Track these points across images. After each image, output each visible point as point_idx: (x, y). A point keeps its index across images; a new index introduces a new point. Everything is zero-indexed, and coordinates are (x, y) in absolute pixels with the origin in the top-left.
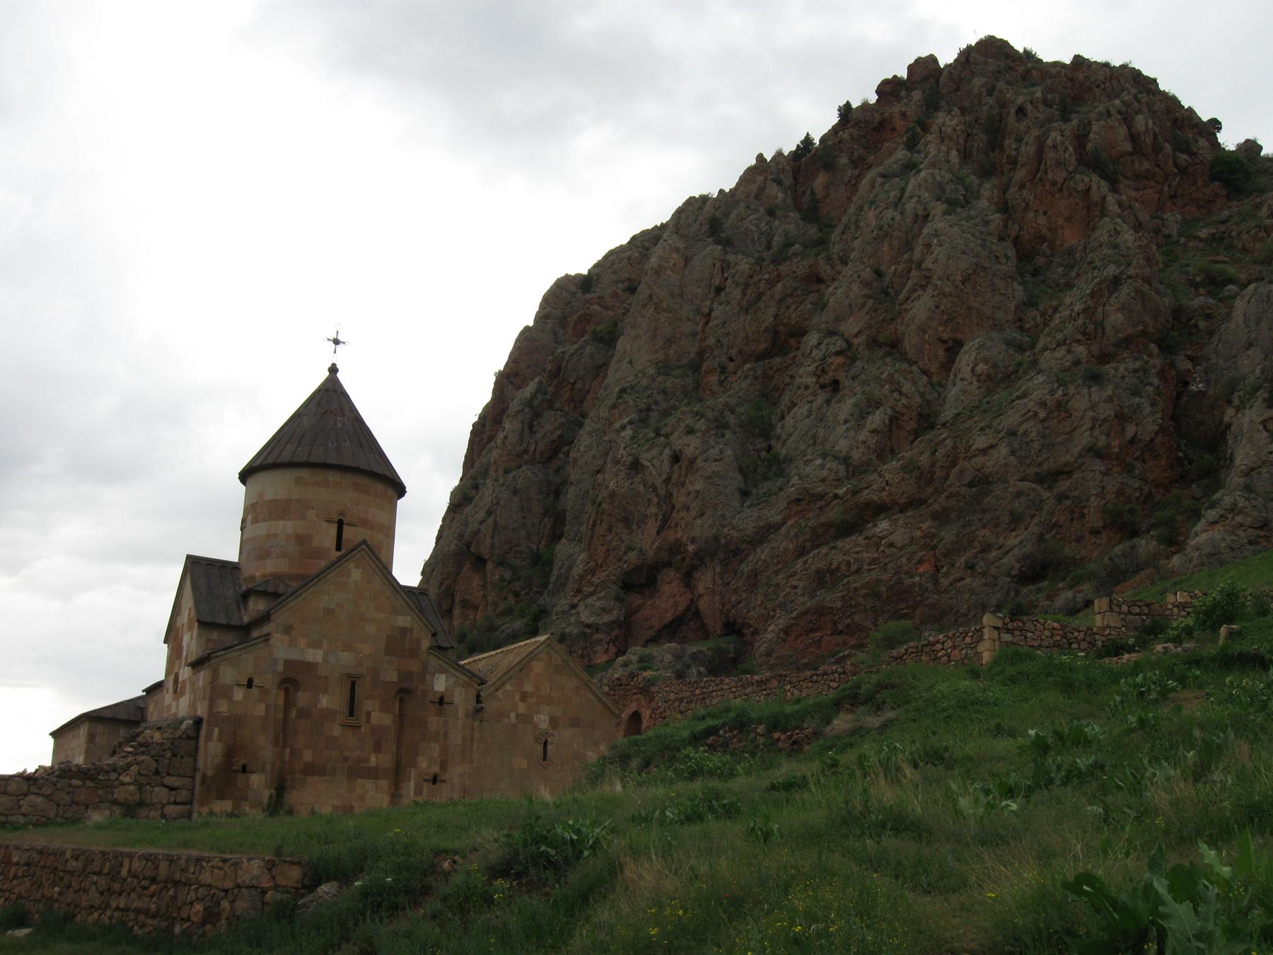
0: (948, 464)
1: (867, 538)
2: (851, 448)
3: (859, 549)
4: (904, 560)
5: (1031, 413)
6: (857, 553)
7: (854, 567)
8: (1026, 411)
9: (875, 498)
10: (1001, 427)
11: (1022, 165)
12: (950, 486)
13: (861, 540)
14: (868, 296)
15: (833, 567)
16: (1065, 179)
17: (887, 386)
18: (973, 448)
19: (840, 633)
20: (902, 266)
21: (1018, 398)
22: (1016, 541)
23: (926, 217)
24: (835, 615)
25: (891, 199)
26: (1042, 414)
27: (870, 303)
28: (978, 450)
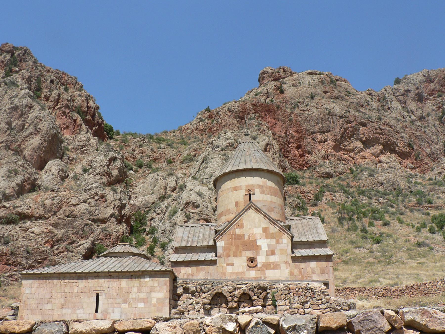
0: (58, 206)
1: (20, 227)
2: (6, 188)
3: (17, 231)
4: (40, 239)
5: (92, 196)
6: (16, 232)
7: (15, 238)
8: (90, 195)
9: (24, 212)
10: (81, 198)
11: (52, 101)
12: (60, 215)
13: (17, 227)
14: (8, 129)
15: (5, 236)
16: (68, 113)
17: (21, 168)
18: (70, 203)
19: (9, 265)
20: (20, 123)
21: (88, 189)
22: (84, 242)
23: (31, 108)
24: (8, 256)
25: (14, 94)
26: (96, 198)
27: (8, 132)
28: (72, 204)
